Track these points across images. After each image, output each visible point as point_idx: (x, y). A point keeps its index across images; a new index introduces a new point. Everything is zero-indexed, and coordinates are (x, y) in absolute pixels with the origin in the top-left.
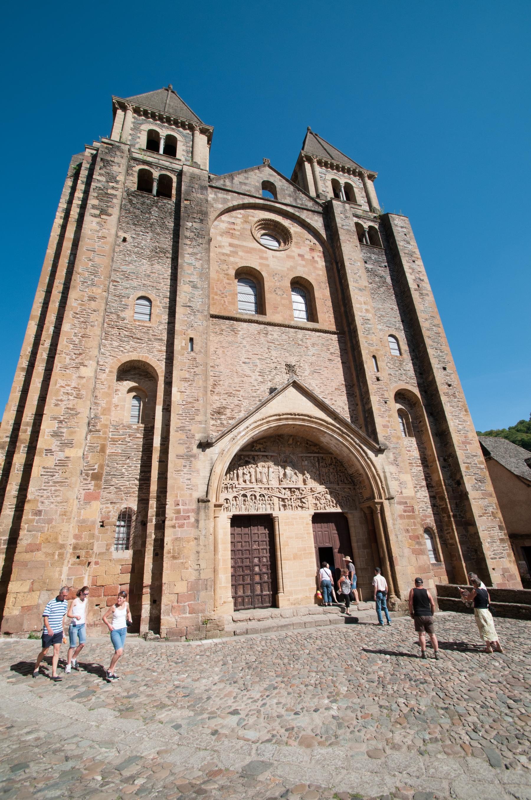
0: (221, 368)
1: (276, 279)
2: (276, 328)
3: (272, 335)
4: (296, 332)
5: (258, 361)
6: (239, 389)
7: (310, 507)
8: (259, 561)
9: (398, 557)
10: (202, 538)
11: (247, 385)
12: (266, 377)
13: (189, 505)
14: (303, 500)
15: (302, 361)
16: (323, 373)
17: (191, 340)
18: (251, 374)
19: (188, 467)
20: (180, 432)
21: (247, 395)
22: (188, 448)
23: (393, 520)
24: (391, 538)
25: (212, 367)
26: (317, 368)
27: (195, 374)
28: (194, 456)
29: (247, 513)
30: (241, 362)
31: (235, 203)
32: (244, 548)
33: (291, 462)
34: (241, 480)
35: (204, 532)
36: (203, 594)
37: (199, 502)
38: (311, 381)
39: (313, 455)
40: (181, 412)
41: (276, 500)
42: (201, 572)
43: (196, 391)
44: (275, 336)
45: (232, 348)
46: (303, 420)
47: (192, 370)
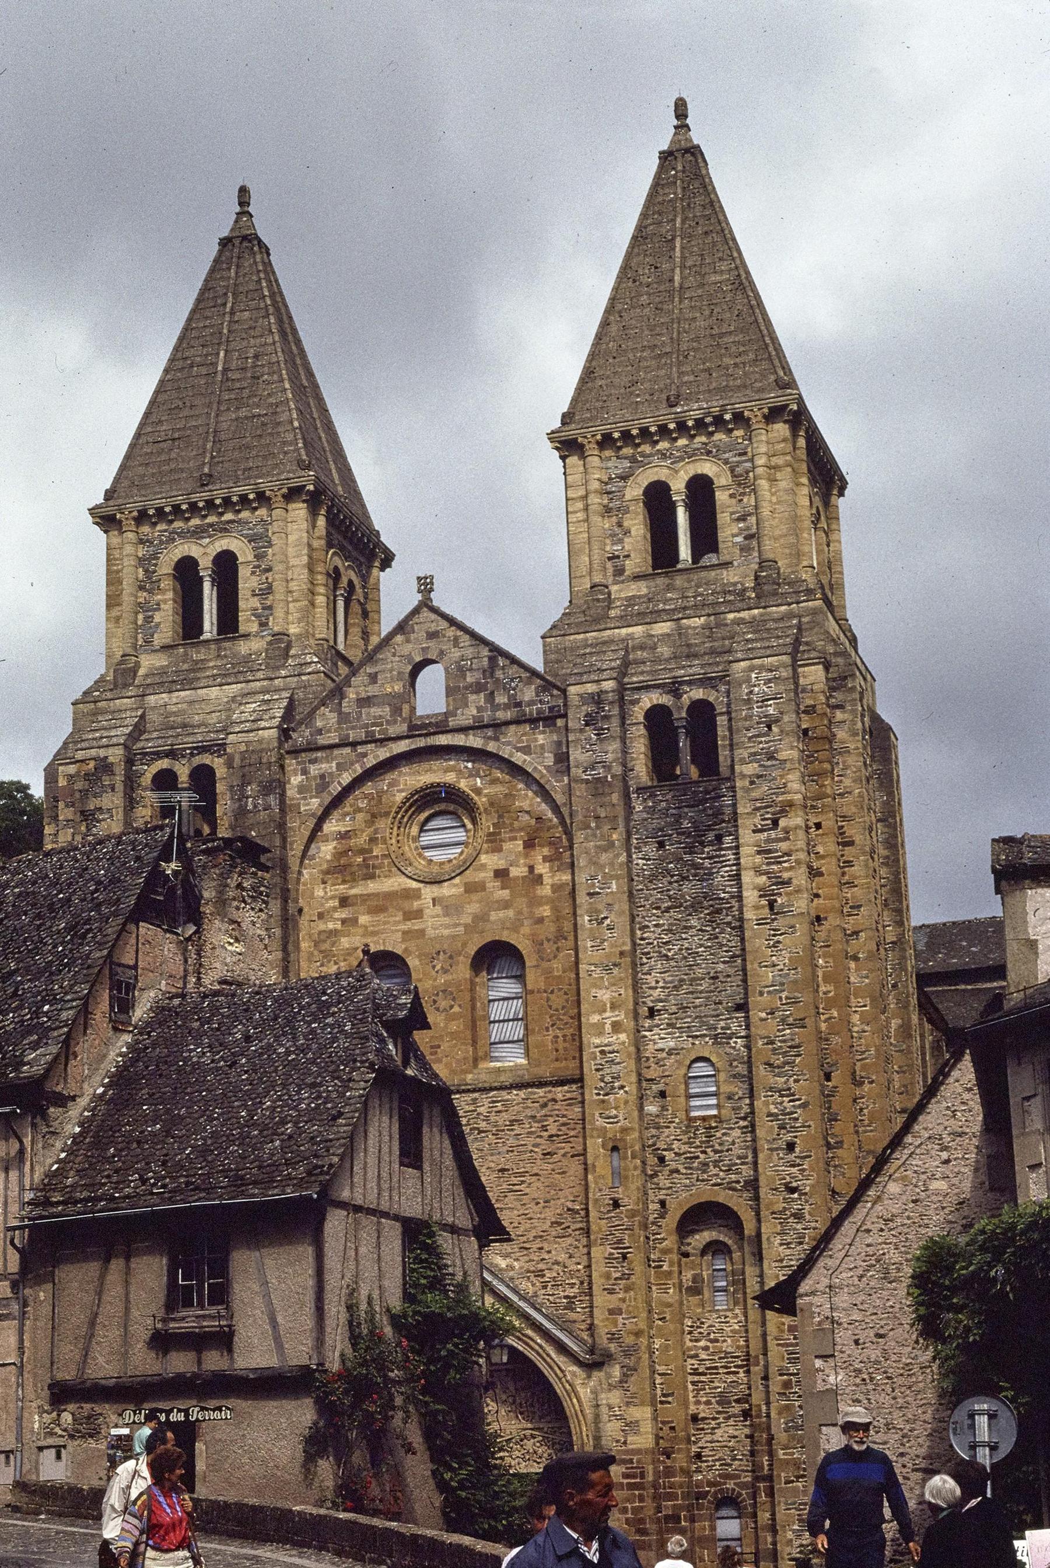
1: (438, 967)
16: (527, 1190)
26: (515, 1180)
31: (346, 778)
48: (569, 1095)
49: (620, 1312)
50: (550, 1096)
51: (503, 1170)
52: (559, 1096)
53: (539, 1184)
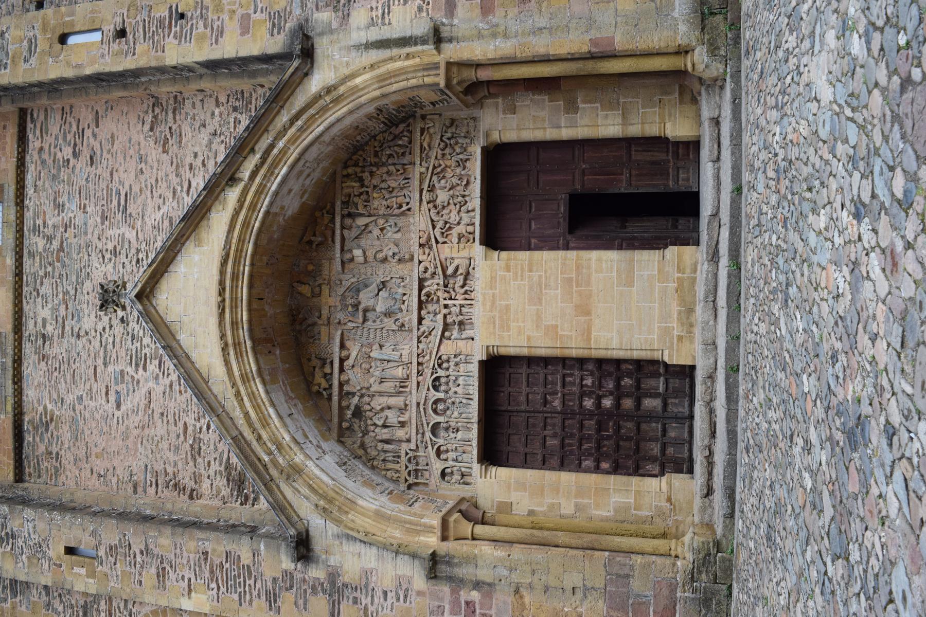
0: (137, 465)
2: (26, 307)
3: (44, 321)
4: (32, 255)
5: (110, 368)
6: (181, 425)
7: (465, 253)
8: (589, 394)
9: (594, 34)
10: (515, 577)
11: (172, 404)
12: (147, 351)
13: (442, 599)
14: (450, 271)
15: (100, 245)
17: (70, 551)
18: (144, 391)
19: (358, 594)
20: (279, 603)
21: (195, 408)
22: (314, 588)
23: (494, 35)
24: (542, 51)
25: (135, 492)
26: (115, 202)
27: (146, 551)
28: (333, 576)
29: (475, 426)
30: (117, 414)
32: (558, 430)
33: (358, 291)
34: (400, 434)
35: (506, 572)
36: (636, 585)
37: (435, 577)
38: (149, 222)
39: (338, 232)
40: (236, 597)
41: (448, 348)
42: (589, 584)
43: (185, 554)
44: (45, 313)
45: (87, 432)
46: (235, 277)
47: (139, 559)
48: (38, 132)
49: (246, 18)
50: (36, 157)
51: (104, 218)
52: (38, 144)
53: (122, 169)
